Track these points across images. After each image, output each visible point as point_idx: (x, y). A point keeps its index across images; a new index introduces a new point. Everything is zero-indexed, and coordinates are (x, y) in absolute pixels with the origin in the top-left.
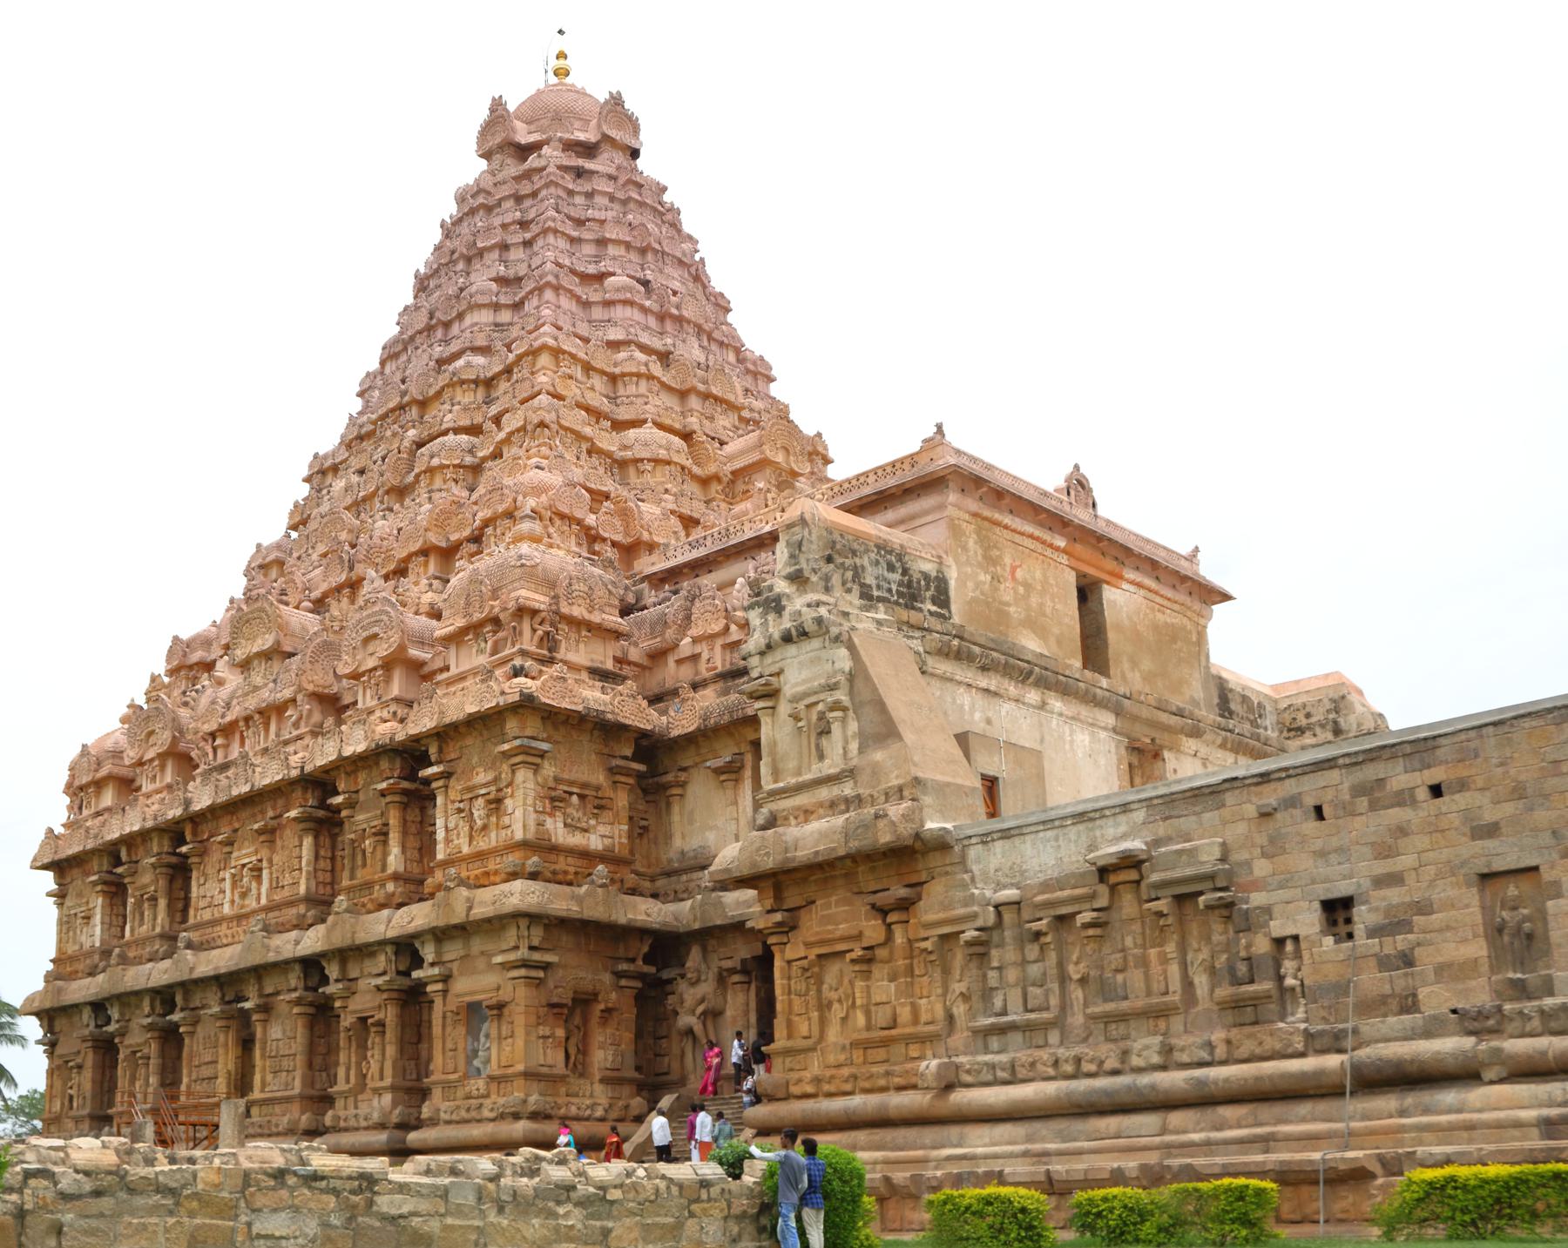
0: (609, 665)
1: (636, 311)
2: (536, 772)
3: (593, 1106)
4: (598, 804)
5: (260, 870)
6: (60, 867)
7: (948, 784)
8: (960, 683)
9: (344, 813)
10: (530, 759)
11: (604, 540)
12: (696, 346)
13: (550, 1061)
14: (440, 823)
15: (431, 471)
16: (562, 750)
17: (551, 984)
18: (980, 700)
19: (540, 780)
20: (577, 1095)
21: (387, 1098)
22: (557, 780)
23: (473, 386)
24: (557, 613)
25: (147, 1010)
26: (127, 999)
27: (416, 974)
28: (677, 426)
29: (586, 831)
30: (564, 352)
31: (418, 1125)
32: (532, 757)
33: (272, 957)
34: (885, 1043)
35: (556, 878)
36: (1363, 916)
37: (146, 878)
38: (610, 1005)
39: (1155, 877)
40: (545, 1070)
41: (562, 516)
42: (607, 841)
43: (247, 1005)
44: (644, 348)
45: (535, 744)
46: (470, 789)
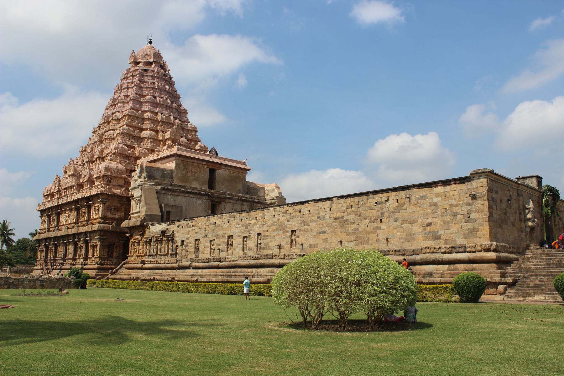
0: (123, 184)
4: (117, 209)
6: (42, 212)
8: (168, 194)
9: (80, 208)
11: (131, 157)
13: (104, 255)
14: (92, 212)
15: (106, 139)
18: (173, 197)
21: (83, 260)
22: (109, 206)
25: (52, 241)
26: (50, 239)
27: (87, 239)
31: (85, 265)
32: (103, 202)
34: (139, 256)
36: (185, 243)
39: (166, 234)
40: (103, 256)
42: (119, 216)
43: (65, 241)
46: (95, 207)
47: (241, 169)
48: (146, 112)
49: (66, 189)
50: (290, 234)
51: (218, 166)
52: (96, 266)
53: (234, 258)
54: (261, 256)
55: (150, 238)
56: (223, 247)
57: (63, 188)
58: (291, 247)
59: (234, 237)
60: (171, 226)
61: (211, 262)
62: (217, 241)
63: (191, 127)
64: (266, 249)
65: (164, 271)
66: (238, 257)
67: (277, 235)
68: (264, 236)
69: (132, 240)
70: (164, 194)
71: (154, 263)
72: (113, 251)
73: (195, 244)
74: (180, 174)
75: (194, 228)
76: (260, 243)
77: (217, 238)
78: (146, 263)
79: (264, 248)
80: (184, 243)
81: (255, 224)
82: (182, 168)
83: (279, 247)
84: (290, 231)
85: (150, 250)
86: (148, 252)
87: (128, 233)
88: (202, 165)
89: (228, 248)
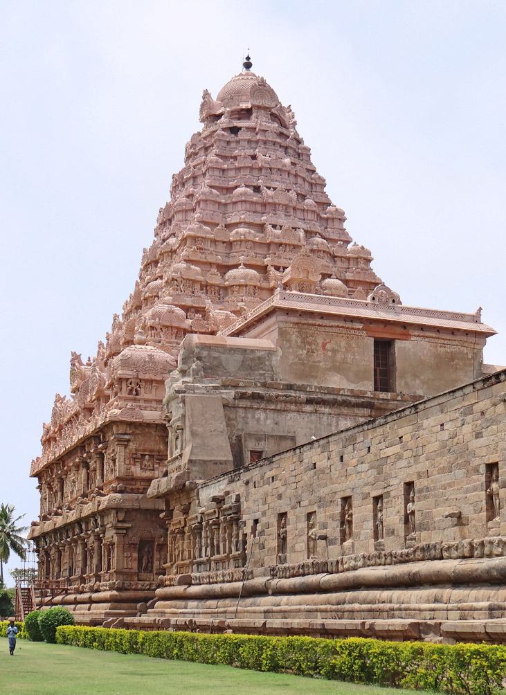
1: (248, 205)
2: (125, 448)
3: (150, 585)
5: (75, 482)
6: (38, 475)
7: (211, 461)
8: (258, 409)
10: (121, 443)
12: (283, 216)
13: (130, 567)
15: (146, 299)
16: (140, 438)
17: (130, 535)
18: (271, 415)
19: (128, 451)
20: (145, 580)
23: (170, 254)
24: (137, 378)
27: (96, 530)
28: (259, 263)
29: (153, 470)
30: (198, 237)
33: (69, 521)
35: (132, 491)
36: (259, 527)
37: (56, 482)
38: (161, 543)
39: (224, 507)
40: (127, 570)
41: (167, 327)
43: (69, 540)
44: (249, 225)
45: (122, 437)
47: (467, 333)
48: (237, 225)
49: (69, 421)
50: (483, 479)
51: (399, 330)
52: (107, 594)
53: (355, 560)
54: (415, 552)
55: (199, 520)
56: (333, 530)
57: (66, 420)
58: (490, 519)
59: (355, 503)
60: (234, 484)
61: (308, 574)
62: (320, 517)
63: (353, 251)
64: (425, 529)
65: (221, 602)
66: (364, 557)
67: (450, 485)
68: (421, 491)
69: (172, 528)
70: (245, 408)
71: (205, 581)
72: (152, 558)
73: (279, 527)
74: (291, 357)
75: (277, 483)
76: (413, 513)
77: (319, 507)
78: (193, 582)
79: (424, 527)
80: (258, 525)
81: (399, 457)
82: (296, 342)
83: (459, 519)
84: (483, 469)
85: (200, 550)
86: (197, 554)
87: (162, 511)
88: (352, 332)
89: (343, 534)
